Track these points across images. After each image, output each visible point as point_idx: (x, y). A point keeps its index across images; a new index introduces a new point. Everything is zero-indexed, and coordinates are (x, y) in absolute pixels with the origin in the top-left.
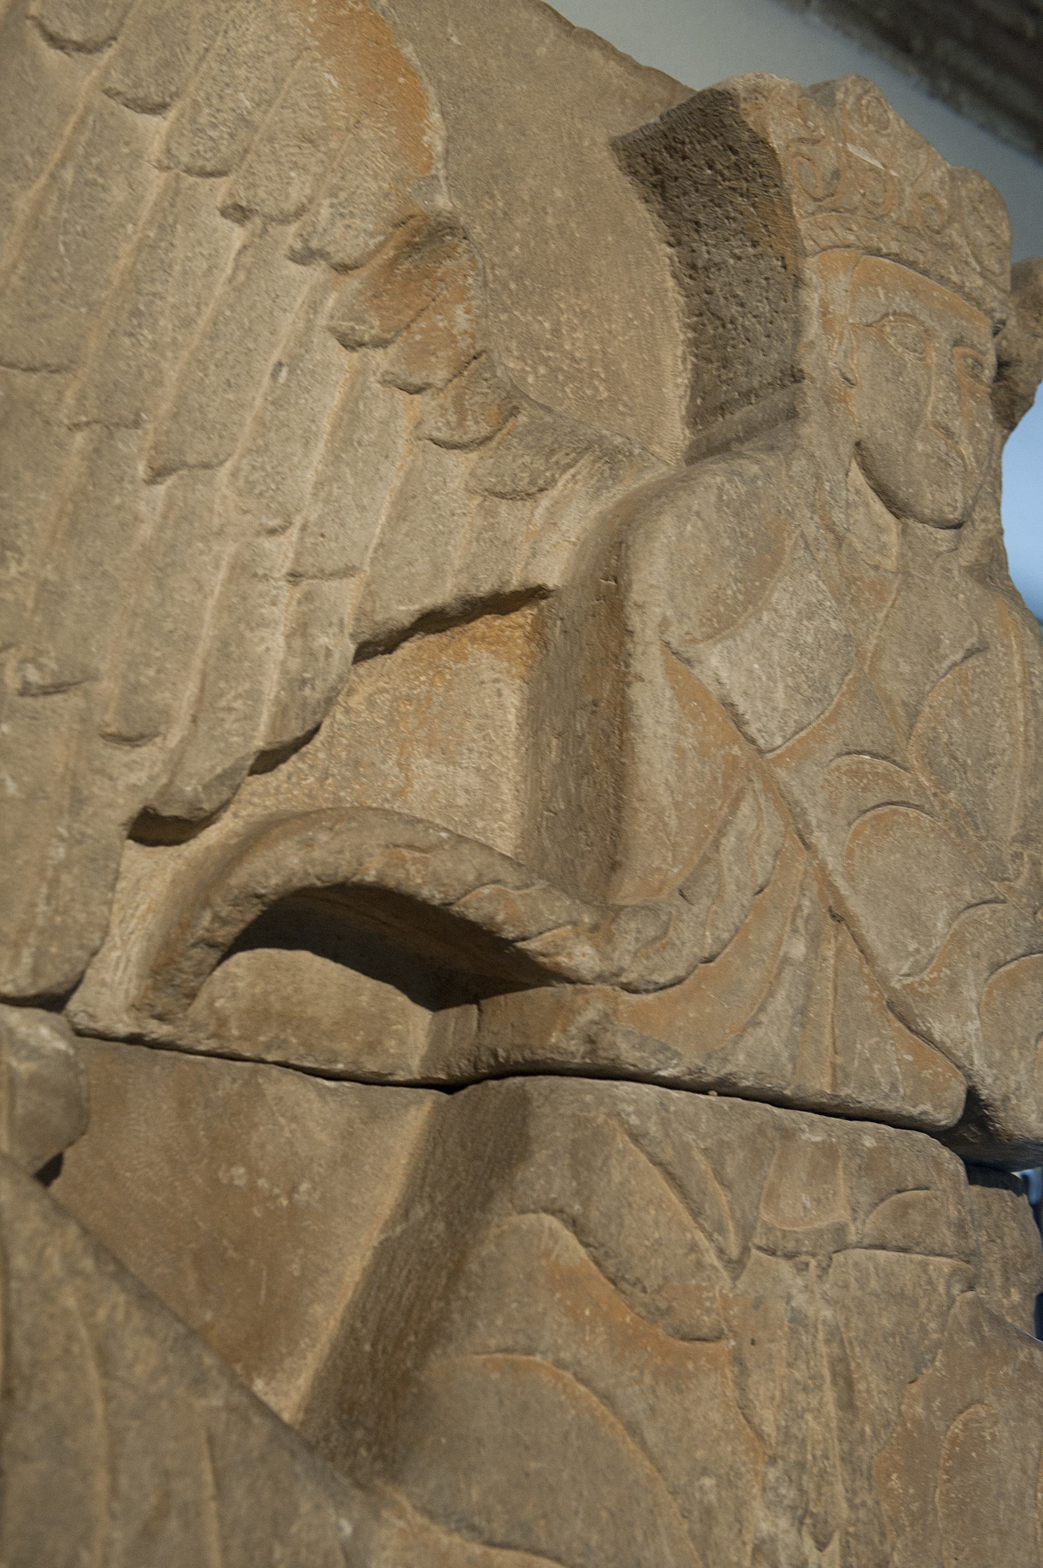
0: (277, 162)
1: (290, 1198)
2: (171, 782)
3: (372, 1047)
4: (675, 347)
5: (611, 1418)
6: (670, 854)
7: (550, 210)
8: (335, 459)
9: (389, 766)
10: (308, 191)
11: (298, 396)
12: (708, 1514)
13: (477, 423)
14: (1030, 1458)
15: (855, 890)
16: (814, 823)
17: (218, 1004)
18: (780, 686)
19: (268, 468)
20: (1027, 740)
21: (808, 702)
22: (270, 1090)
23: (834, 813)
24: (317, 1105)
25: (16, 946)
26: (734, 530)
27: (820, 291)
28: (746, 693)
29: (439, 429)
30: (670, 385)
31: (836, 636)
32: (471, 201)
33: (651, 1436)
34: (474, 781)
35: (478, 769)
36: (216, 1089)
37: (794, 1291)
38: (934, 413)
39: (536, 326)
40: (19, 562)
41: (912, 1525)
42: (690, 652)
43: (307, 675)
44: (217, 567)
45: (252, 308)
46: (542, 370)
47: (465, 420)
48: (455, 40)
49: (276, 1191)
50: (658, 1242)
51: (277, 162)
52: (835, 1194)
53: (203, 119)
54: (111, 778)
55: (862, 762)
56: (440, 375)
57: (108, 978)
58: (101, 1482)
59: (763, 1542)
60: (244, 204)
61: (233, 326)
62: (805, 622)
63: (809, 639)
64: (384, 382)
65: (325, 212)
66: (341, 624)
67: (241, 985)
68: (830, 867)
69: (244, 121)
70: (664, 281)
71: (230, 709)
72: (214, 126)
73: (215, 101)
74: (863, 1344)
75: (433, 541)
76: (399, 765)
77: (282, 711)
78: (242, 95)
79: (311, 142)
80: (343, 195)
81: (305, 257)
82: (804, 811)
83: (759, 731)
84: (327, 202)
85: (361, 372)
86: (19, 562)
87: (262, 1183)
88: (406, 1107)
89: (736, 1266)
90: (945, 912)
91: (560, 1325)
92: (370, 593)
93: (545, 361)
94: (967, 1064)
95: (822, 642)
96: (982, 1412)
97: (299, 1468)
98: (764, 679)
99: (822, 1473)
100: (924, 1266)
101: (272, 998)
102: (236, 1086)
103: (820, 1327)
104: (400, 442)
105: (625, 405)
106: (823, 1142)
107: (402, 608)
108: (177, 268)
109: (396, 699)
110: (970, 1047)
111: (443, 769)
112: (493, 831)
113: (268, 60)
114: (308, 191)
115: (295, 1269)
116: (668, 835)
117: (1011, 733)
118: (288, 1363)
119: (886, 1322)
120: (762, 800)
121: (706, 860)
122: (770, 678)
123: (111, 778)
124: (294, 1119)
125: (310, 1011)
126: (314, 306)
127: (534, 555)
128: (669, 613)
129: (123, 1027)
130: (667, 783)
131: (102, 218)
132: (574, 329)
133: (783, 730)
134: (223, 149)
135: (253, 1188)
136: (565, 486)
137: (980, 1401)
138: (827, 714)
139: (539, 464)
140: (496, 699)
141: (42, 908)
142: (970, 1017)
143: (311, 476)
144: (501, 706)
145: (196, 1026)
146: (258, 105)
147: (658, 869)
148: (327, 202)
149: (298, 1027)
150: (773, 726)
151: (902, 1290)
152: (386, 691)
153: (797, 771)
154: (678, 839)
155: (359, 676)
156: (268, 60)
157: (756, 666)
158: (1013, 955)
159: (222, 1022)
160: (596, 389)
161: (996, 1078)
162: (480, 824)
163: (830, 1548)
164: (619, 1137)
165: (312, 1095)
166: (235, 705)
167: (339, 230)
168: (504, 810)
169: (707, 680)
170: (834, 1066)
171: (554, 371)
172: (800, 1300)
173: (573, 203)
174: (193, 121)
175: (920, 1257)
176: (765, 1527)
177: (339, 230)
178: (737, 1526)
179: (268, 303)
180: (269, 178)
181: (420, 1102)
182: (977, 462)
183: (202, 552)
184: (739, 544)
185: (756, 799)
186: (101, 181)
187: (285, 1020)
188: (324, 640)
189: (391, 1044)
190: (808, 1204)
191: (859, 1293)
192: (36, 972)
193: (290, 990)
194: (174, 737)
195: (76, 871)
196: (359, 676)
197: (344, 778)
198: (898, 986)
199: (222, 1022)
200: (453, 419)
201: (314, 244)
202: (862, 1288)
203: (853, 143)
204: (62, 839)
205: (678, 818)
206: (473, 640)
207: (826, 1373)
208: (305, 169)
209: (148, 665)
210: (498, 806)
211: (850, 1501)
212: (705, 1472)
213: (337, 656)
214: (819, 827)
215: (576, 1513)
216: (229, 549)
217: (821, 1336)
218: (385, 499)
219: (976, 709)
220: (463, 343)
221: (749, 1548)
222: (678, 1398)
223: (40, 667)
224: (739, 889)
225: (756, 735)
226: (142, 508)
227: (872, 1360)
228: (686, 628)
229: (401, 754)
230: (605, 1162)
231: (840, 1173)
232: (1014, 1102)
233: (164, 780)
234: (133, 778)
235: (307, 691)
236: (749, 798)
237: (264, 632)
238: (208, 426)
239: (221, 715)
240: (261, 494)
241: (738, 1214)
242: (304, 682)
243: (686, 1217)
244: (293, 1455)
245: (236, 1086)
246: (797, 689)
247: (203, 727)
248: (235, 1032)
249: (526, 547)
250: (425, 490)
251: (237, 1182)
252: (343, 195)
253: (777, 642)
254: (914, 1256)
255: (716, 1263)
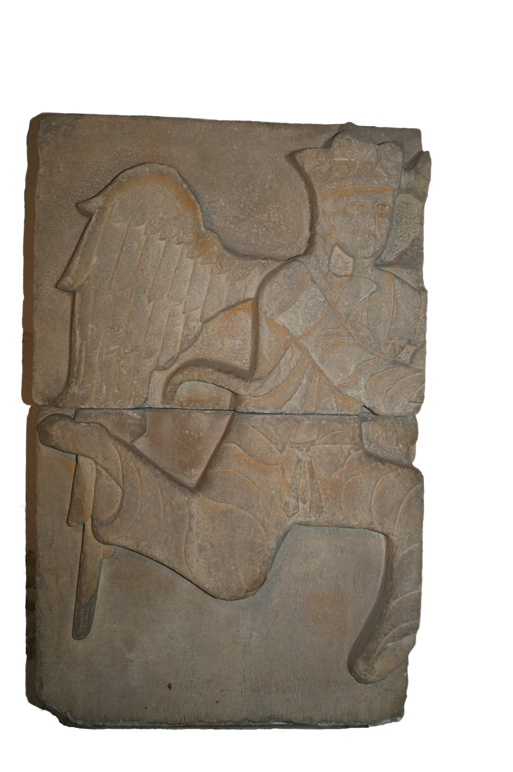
0: (170, 226)
1: (198, 436)
2: (158, 364)
3: (217, 404)
4: (307, 209)
5: (249, 480)
6: (267, 365)
7: (267, 183)
8: (191, 285)
9: (219, 343)
10: (177, 230)
11: (181, 274)
12: (272, 497)
13: (226, 267)
14: (371, 487)
15: (323, 365)
16: (310, 351)
17: (180, 400)
18: (301, 320)
19: (176, 292)
20: (393, 312)
21: (310, 321)
22: (193, 415)
23: (317, 347)
24: (204, 417)
25: (129, 400)
26: (288, 283)
27: (321, 207)
28: (289, 324)
29: (217, 271)
30: (306, 220)
31: (321, 302)
32: (241, 191)
33: (257, 484)
34: (241, 342)
35: (242, 340)
36: (181, 416)
37: (299, 455)
38: (364, 227)
39: (262, 218)
40: (122, 329)
41: (332, 500)
42: (273, 318)
43: (188, 334)
44: (166, 316)
45: (169, 258)
46: (264, 229)
47: (223, 267)
48: (236, 148)
49: (195, 435)
50: (261, 448)
51: (170, 226)
52: (313, 434)
53: (152, 223)
54: (145, 365)
55: (329, 332)
56: (215, 260)
57: (156, 398)
58: (140, 491)
59: (286, 502)
60: (164, 237)
61: (164, 264)
62: (310, 301)
63: (311, 305)
64: (201, 264)
65: (181, 234)
66: (197, 320)
67: (185, 395)
68: (315, 360)
69: (162, 219)
70: (303, 191)
71: (170, 346)
72: (155, 223)
73: (155, 218)
74: (320, 465)
75: (219, 296)
76: (221, 343)
77: (182, 343)
78: (161, 214)
79: (177, 219)
80: (184, 229)
81: (179, 243)
82: (307, 349)
83: (293, 332)
84: (181, 232)
85: (195, 264)
86: (122, 329)
87: (192, 433)
88: (226, 415)
89: (281, 451)
90: (354, 365)
91: (235, 464)
92: (203, 312)
93: (265, 226)
94: (360, 401)
95: (316, 305)
96: (358, 477)
97: (176, 489)
98: (295, 319)
99: (305, 490)
100: (341, 448)
101: (193, 397)
102: (185, 415)
103: (306, 462)
104: (208, 276)
105: (291, 230)
106: (310, 423)
107: (212, 313)
108: (151, 256)
109: (219, 328)
110: (360, 396)
111: (232, 341)
112: (245, 353)
113: (165, 204)
114: (177, 230)
115: (200, 449)
116: (266, 361)
117: (388, 311)
118: (199, 466)
119: (327, 460)
120: (294, 348)
121: (276, 365)
122: (297, 318)
123: (145, 365)
124: (199, 420)
125: (201, 399)
126: (182, 253)
127: (246, 292)
128: (267, 309)
129: (161, 406)
130: (266, 349)
131: (133, 253)
132: (274, 214)
133: (301, 330)
134: (158, 227)
135: (190, 434)
136: (253, 274)
137: (358, 475)
138: (317, 322)
139: (244, 271)
140: (246, 322)
141: (133, 392)
142: (361, 389)
143: (186, 290)
144: (247, 324)
145: (176, 405)
146: (165, 215)
147: (264, 369)
148: (181, 232)
149: (199, 402)
150: (298, 330)
151: (333, 453)
152: (216, 326)
153: (305, 339)
154: (269, 362)
155: (209, 325)
156: (165, 204)
157: (293, 316)
158: (379, 371)
159: (181, 403)
160: (282, 229)
161: (370, 403)
162: (242, 352)
163: (307, 504)
164: (250, 427)
165: (203, 415)
166: (171, 344)
167: (185, 237)
168: (247, 349)
169: (278, 322)
170: (316, 406)
171: (267, 229)
172: (301, 456)
173: (274, 178)
174: (150, 224)
175: (340, 445)
176: (288, 500)
177: (185, 237)
178: (280, 500)
179: (172, 256)
180: (169, 230)
181: (228, 414)
182: (381, 236)
183: (162, 314)
184: (290, 286)
185: (292, 348)
186: (132, 245)
187: (195, 401)
188: (193, 324)
189: (222, 403)
190: (305, 437)
191: (319, 454)
192: (133, 404)
193: (196, 395)
194: (158, 353)
195: (140, 384)
196: (209, 325)
197: (206, 349)
198: (337, 385)
199: (181, 403)
200: (220, 268)
201: (180, 241)
202: (320, 453)
203: (337, 157)
204: (136, 380)
205: (269, 357)
206: (239, 310)
207: (307, 471)
208: (176, 225)
209: (151, 341)
210: (247, 347)
211: (311, 495)
212: (272, 490)
213: (197, 327)
214: (312, 351)
215: (238, 497)
216: (167, 312)
217: (306, 463)
218: (206, 288)
219: (375, 307)
220: (218, 253)
221: (283, 504)
222: (265, 477)
223: (128, 349)
224: (285, 371)
225: (292, 333)
226: (148, 309)
227: (322, 468)
228: (271, 312)
229: (222, 340)
230: (246, 433)
231: (315, 429)
232: (376, 407)
233: (156, 364)
234: (150, 364)
235: (189, 337)
236: (290, 349)
237: (178, 327)
238: (161, 288)
239: (168, 348)
240: (175, 298)
241: (282, 441)
242: (188, 335)
243: (268, 442)
244: (175, 487)
245: (185, 415)
246: (306, 319)
247: (164, 351)
248: (185, 405)
249: (244, 290)
250: (215, 285)
251: (187, 433)
252: (184, 229)
253: (300, 308)
254: (338, 445)
255: (276, 450)
